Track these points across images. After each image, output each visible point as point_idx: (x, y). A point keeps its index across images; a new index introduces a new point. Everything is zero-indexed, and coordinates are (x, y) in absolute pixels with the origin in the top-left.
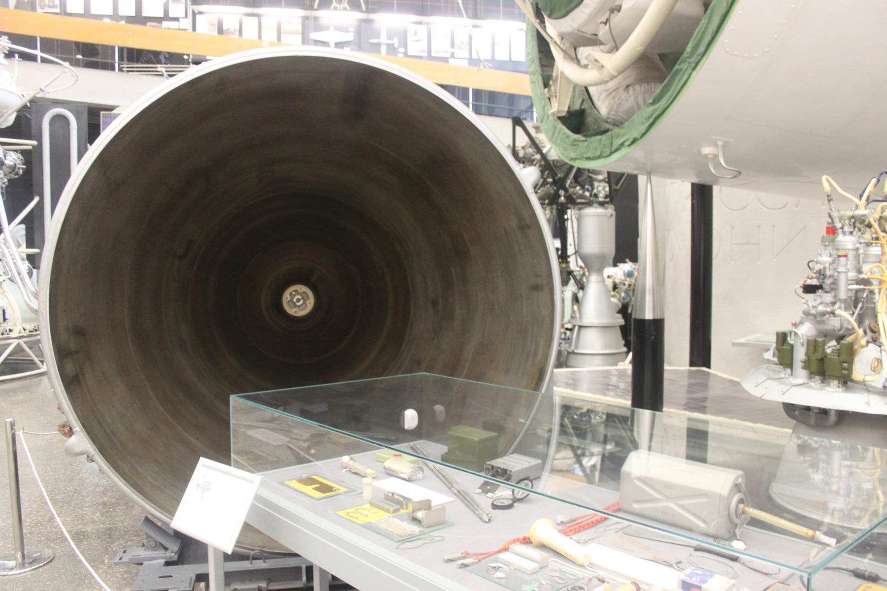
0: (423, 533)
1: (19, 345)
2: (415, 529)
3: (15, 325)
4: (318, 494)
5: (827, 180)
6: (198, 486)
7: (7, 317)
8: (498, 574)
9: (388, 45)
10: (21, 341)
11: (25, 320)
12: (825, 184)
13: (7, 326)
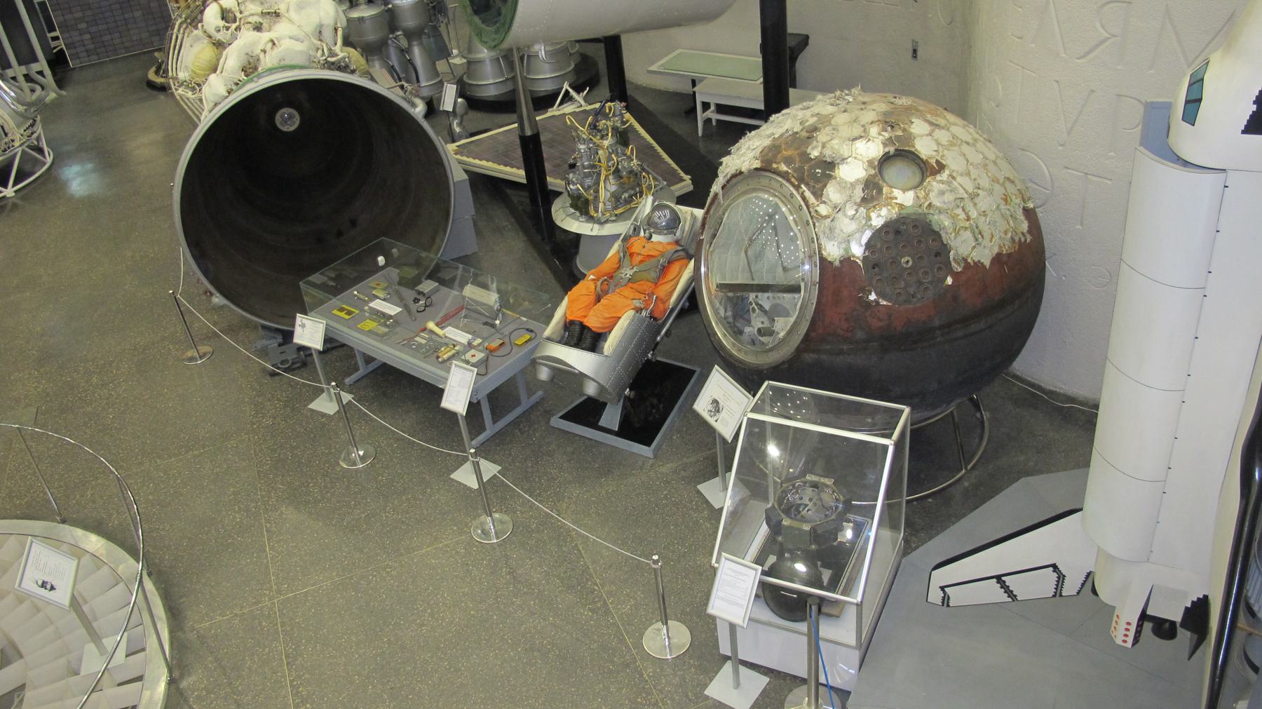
0: (390, 331)
1: (23, 151)
2: (386, 330)
3: (13, 134)
7: (6, 132)
10: (24, 147)
11: (18, 126)
13: (10, 137)
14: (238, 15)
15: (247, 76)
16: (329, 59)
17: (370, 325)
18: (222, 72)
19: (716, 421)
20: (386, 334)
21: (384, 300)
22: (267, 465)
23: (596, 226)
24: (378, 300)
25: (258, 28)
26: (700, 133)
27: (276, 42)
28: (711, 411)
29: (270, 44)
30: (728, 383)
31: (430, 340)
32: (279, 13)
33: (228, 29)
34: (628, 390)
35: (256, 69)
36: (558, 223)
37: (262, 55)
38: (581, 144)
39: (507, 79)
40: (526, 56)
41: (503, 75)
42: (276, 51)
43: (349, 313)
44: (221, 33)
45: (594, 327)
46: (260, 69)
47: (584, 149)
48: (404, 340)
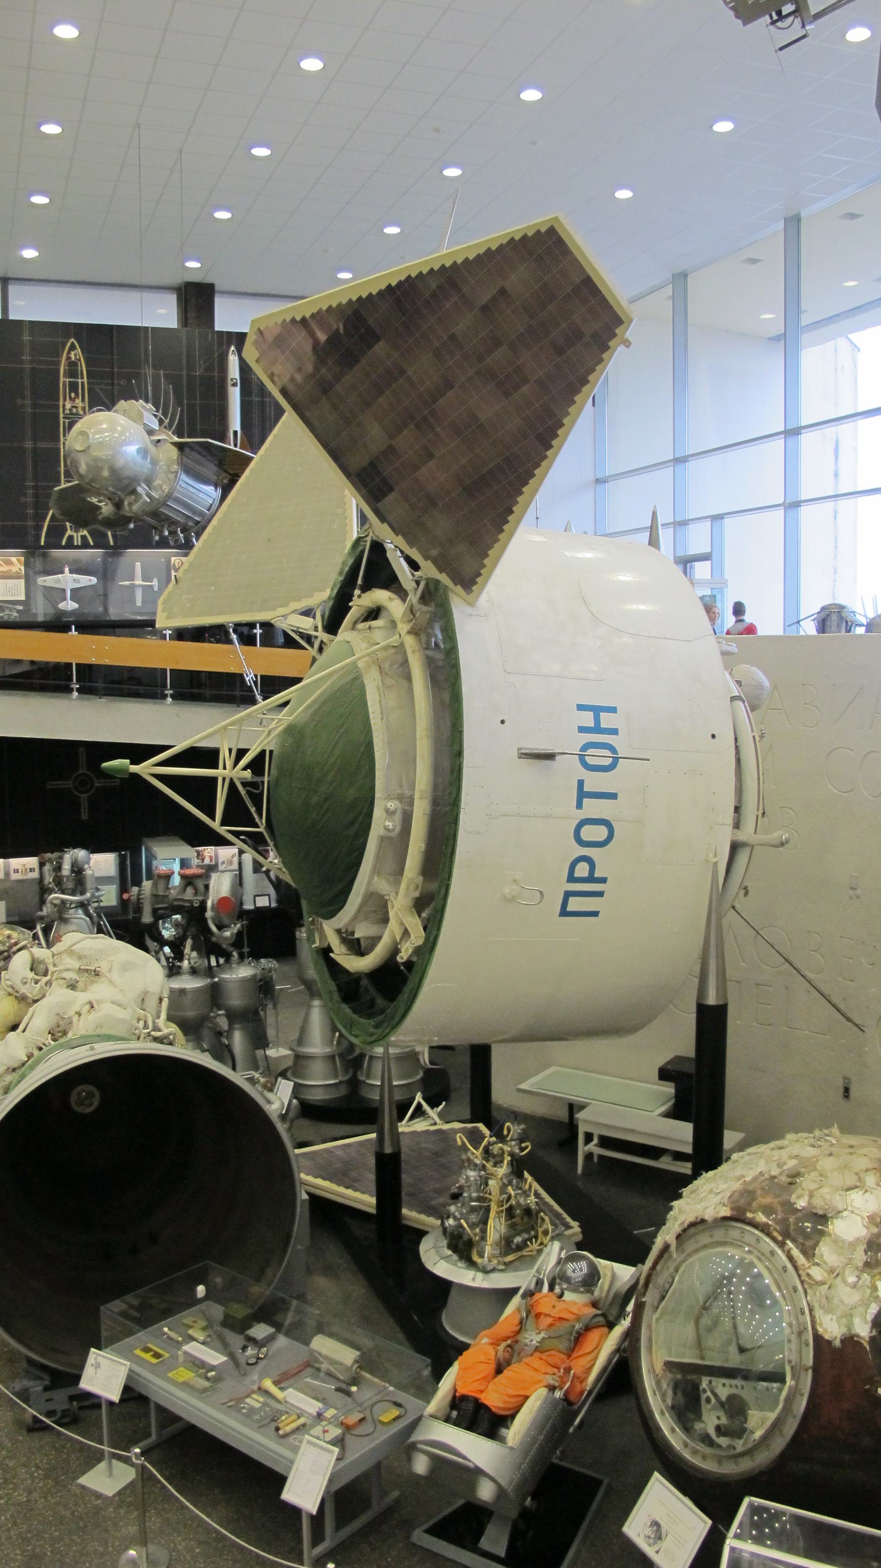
0: (211, 1387)
2: (207, 1384)
4: (154, 1361)
5: (460, 1137)
6: (92, 1365)
8: (244, 1411)
9: (143, 587)
12: (458, 1140)
14: (51, 969)
15: (54, 1040)
16: (153, 1033)
17: (184, 1374)
18: (24, 1031)
19: (657, 1552)
20: (205, 1390)
21: (203, 1343)
22: (16, 1560)
23: (480, 1275)
24: (194, 1343)
25: (73, 986)
26: (580, 1170)
27: (95, 1005)
28: (649, 1537)
29: (88, 1006)
30: (673, 1498)
31: (265, 1404)
32: (99, 972)
33: (37, 982)
34: (529, 1499)
35: (65, 1033)
36: (429, 1266)
37: (75, 1019)
38: (471, 1170)
39: (341, 1082)
40: (367, 1058)
41: (336, 1076)
42: (93, 1016)
43: (157, 1355)
44: (27, 986)
45: (494, 1407)
46: (70, 1035)
47: (474, 1177)
48: (231, 1400)
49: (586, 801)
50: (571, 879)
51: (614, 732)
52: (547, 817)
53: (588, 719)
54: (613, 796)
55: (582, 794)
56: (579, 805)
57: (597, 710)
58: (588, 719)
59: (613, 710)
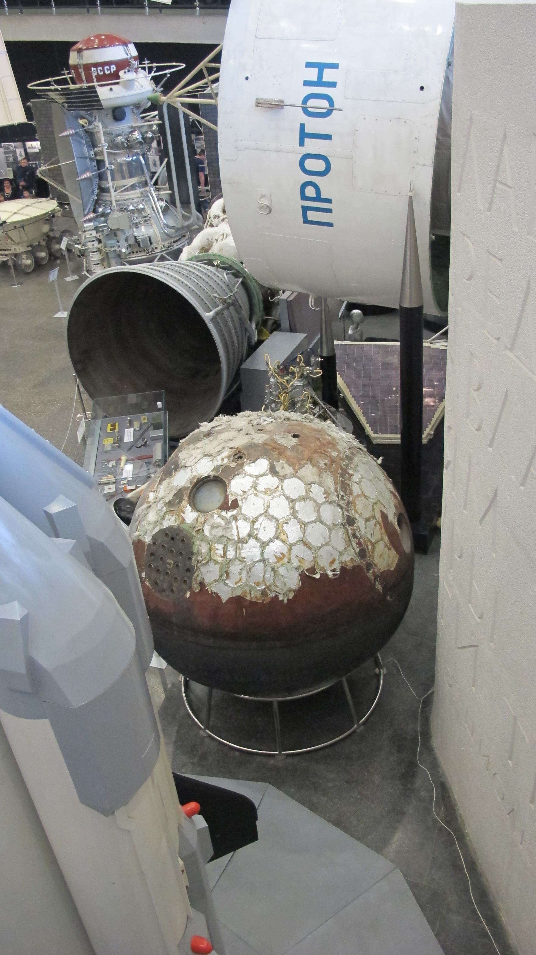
49: (306, 140)
50: (304, 197)
51: (333, 85)
52: (278, 151)
53: (312, 74)
54: (328, 137)
55: (304, 135)
56: (302, 144)
57: (321, 67)
58: (312, 74)
59: (335, 66)
